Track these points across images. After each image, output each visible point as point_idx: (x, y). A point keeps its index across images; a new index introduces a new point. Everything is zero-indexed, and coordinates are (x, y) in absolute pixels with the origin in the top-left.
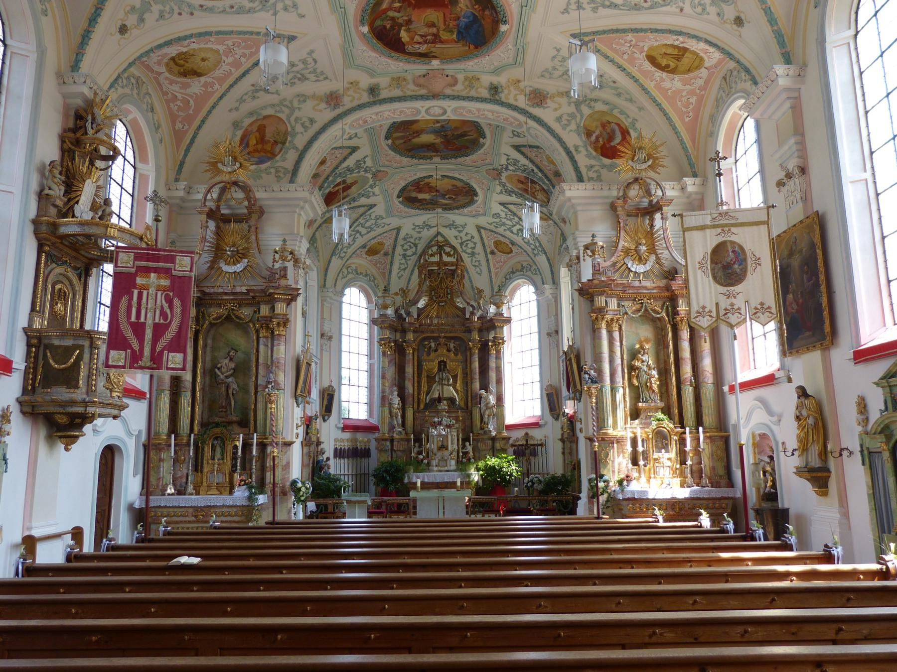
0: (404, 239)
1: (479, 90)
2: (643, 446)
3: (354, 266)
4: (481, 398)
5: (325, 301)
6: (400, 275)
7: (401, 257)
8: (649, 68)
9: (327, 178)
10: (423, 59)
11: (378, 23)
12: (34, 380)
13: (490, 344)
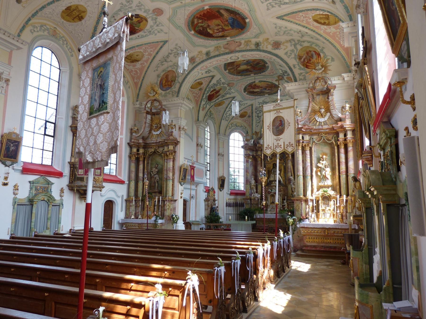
0: (256, 109)
1: (251, 46)
2: (316, 203)
3: (235, 123)
5: (220, 139)
6: (257, 125)
7: (256, 117)
8: (317, 25)
9: (206, 90)
10: (223, 38)
11: (197, 29)
12: (72, 179)
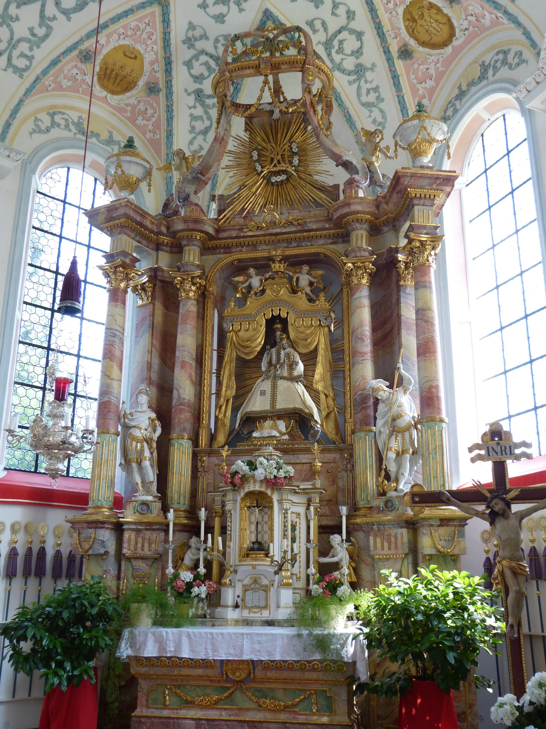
0: (189, 42)
4: (377, 402)
7: (191, 100)
13: (401, 257)
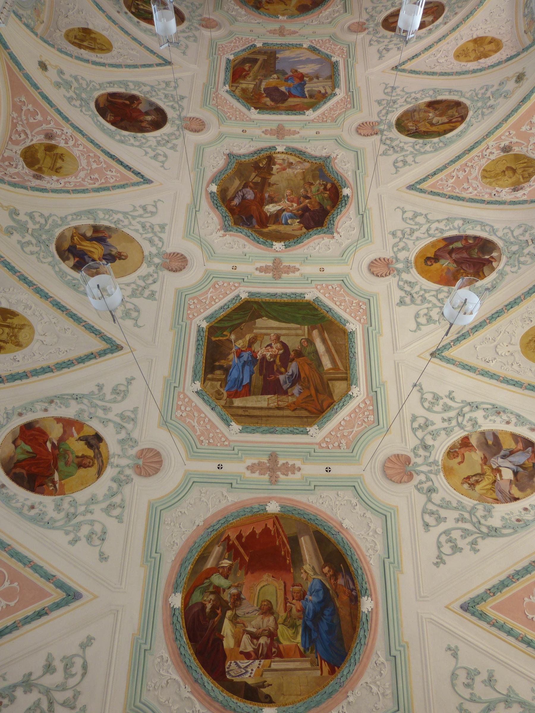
11: (197, 597)
